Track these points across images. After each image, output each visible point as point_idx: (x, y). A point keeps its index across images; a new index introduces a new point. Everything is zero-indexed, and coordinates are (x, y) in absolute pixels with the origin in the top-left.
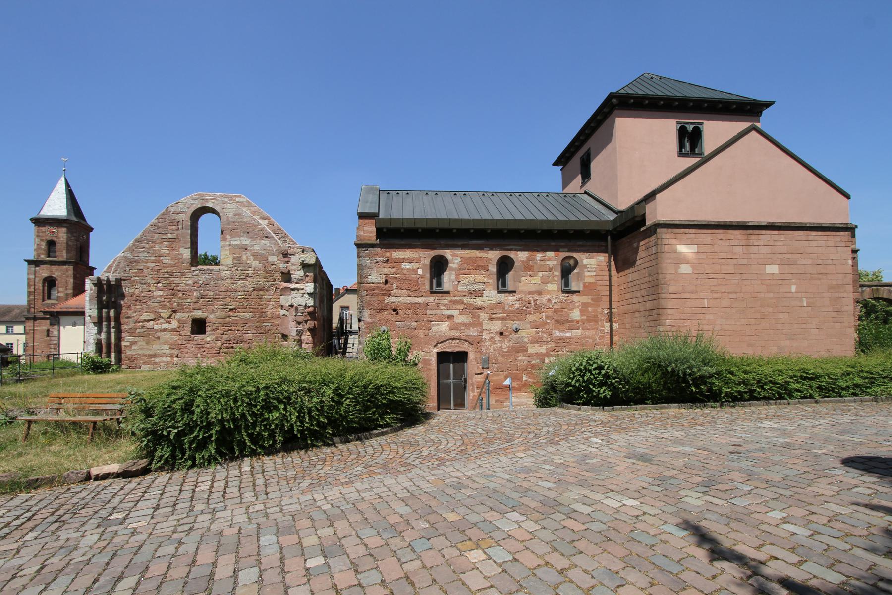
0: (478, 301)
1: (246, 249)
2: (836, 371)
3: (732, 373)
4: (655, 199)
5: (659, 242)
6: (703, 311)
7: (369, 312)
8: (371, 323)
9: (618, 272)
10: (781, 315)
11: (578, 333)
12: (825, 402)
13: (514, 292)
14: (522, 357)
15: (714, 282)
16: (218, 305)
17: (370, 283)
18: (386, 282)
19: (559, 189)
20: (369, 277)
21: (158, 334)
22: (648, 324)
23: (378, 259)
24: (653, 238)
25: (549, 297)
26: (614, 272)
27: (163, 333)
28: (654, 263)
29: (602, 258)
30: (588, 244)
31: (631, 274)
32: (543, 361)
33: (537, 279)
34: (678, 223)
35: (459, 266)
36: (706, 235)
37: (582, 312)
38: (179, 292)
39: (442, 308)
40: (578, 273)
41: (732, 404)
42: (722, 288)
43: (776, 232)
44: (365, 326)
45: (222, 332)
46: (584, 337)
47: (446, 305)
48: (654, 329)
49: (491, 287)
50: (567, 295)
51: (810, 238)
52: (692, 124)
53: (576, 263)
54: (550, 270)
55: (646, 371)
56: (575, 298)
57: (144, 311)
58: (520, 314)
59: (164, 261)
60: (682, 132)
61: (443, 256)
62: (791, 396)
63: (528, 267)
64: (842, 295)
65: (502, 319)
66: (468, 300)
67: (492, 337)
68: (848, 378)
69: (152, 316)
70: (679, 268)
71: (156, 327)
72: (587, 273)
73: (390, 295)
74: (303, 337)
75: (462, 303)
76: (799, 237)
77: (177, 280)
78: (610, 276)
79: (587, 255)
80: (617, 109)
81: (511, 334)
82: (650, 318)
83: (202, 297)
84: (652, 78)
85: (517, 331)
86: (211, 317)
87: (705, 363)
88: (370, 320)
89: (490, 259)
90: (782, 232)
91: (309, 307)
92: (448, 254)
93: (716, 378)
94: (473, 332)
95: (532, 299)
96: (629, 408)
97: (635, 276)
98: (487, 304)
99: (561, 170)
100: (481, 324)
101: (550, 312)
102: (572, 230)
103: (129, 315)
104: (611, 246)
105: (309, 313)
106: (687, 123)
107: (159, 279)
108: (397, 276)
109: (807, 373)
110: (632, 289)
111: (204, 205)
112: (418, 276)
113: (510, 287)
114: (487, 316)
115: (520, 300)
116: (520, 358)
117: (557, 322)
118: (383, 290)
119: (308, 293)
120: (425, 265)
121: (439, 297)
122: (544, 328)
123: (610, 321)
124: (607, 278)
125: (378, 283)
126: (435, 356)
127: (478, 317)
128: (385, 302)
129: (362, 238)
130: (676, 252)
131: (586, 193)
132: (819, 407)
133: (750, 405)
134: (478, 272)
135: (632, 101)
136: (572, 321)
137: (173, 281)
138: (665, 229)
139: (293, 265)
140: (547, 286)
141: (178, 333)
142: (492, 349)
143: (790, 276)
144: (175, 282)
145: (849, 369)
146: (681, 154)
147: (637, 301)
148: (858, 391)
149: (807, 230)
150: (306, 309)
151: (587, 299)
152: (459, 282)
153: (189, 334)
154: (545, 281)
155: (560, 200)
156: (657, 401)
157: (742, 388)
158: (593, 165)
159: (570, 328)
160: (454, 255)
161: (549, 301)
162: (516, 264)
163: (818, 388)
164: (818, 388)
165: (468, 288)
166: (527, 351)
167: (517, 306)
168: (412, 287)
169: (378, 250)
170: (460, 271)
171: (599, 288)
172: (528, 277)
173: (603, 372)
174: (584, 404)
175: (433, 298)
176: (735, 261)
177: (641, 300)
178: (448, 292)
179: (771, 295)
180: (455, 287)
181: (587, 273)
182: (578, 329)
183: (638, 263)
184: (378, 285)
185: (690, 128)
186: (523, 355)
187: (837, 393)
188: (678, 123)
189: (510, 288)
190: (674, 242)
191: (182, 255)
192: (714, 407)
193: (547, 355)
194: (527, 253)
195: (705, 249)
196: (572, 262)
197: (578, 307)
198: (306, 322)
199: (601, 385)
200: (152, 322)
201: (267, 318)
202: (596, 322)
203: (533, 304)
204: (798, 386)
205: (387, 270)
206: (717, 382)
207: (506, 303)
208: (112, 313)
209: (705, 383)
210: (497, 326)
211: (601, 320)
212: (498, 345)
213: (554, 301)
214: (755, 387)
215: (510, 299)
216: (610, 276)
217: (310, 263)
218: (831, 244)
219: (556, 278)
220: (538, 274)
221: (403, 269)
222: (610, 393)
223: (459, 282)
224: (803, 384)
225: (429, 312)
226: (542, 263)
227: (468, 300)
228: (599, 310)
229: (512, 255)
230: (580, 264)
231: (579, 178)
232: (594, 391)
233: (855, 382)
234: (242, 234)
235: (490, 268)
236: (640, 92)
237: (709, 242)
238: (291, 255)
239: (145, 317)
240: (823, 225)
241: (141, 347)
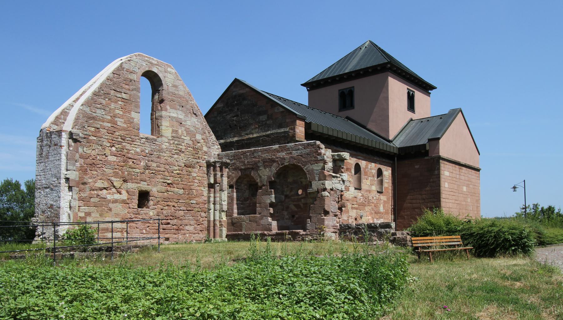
16: (159, 179)
21: (111, 205)
27: (115, 205)
30: (384, 160)
38: (130, 160)
45: (162, 207)
57: (99, 178)
59: (119, 123)
69: (106, 185)
71: (109, 197)
77: (128, 146)
83: (147, 167)
86: (154, 190)
90: (468, 169)
103: (85, 181)
107: (114, 142)
111: (151, 69)
137: (125, 146)
141: (128, 205)
144: (127, 148)
153: (136, 207)
191: (133, 118)
200: (105, 191)
201: (193, 196)
234: (178, 107)
239: (99, 184)
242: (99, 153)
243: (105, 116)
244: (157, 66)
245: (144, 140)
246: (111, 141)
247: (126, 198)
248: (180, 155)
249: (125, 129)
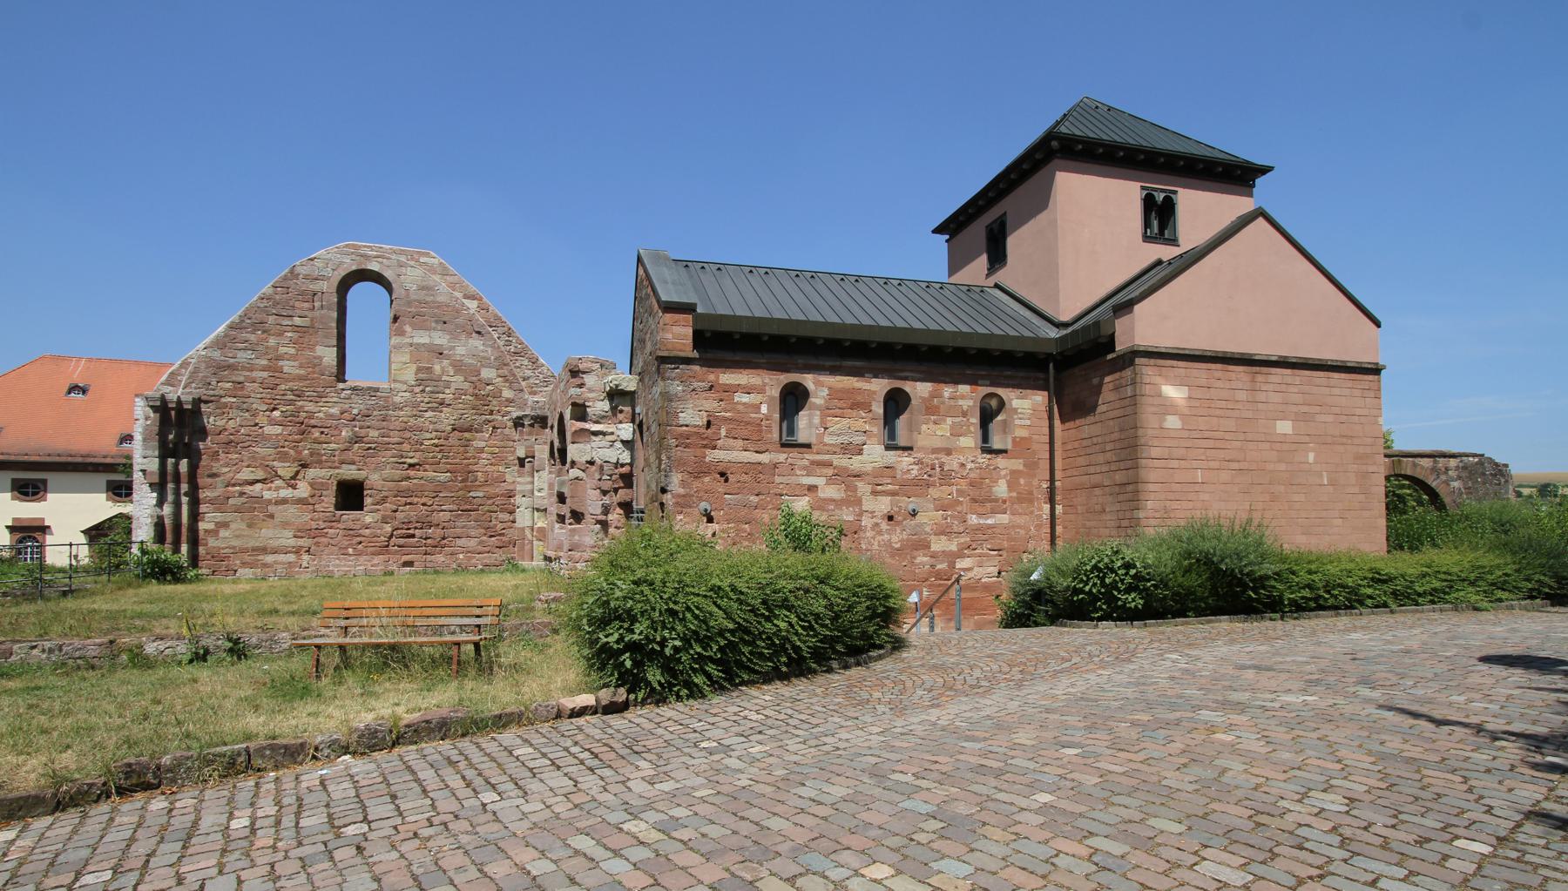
0: (855, 463)
1: (441, 354)
2: (1411, 571)
3: (1293, 573)
4: (1131, 312)
5: (1138, 380)
6: (1197, 487)
7: (680, 476)
8: (684, 496)
9: (1063, 421)
10: (1296, 498)
12: (1401, 611)
13: (911, 449)
14: (922, 558)
15: (1211, 443)
16: (387, 457)
17: (681, 426)
18: (709, 424)
19: (942, 275)
20: (680, 415)
21: (272, 509)
22: (1118, 507)
23: (696, 384)
24: (1128, 373)
25: (962, 460)
26: (1057, 422)
27: (280, 507)
28: (1129, 410)
29: (1039, 398)
30: (1021, 374)
31: (1086, 427)
32: (952, 565)
33: (944, 429)
34: (1163, 350)
35: (826, 402)
36: (1199, 371)
37: (1010, 486)
38: (313, 430)
39: (798, 472)
40: (1004, 421)
41: (1295, 615)
42: (1221, 454)
43: (1289, 371)
44: (674, 500)
45: (394, 507)
46: (1013, 526)
47: (805, 468)
48: (1128, 515)
49: (875, 440)
50: (989, 456)
51: (1333, 382)
52: (1163, 191)
53: (1002, 404)
54: (964, 414)
55: (1188, 570)
56: (1000, 461)
57: (245, 464)
58: (918, 486)
59: (286, 369)
60: (1149, 202)
61: (800, 384)
62: (1362, 603)
63: (931, 409)
64: (1371, 469)
65: (893, 494)
66: (840, 461)
67: (877, 525)
68: (1424, 581)
69: (260, 474)
70: (1165, 420)
71: (267, 495)
72: (1017, 422)
73: (714, 448)
74: (610, 517)
75: (829, 464)
76: (1318, 381)
77: (310, 407)
78: (1051, 427)
79: (1018, 392)
80: (1058, 158)
81: (905, 519)
82: (1121, 498)
83: (357, 439)
84: (1097, 107)
85: (914, 514)
86: (374, 480)
87: (1263, 556)
88: (682, 491)
89: (874, 393)
91: (623, 465)
92: (808, 380)
93: (1275, 579)
94: (847, 515)
95: (936, 461)
96: (1167, 623)
97: (1096, 430)
98: (869, 468)
99: (947, 241)
100: (859, 502)
101: (963, 485)
102: (998, 350)
103: (214, 470)
104: (1055, 379)
105: (622, 476)
106: (1156, 190)
107: (275, 402)
108: (728, 414)
109: (1379, 574)
110: (1089, 451)
111: (363, 267)
112: (761, 416)
113: (902, 441)
114: (869, 488)
115: (919, 462)
116: (919, 560)
117: (974, 500)
118: (704, 439)
119: (622, 441)
120: (772, 398)
121: (794, 453)
122: (955, 510)
123: (1052, 501)
124: (1046, 430)
125: (696, 426)
127: (855, 489)
128: (707, 459)
129: (670, 347)
130: (1160, 395)
131: (997, 286)
132: (1399, 618)
133: (1317, 617)
134: (854, 413)
135: (1080, 147)
136: (996, 500)
137: (302, 407)
138: (1147, 360)
139: (591, 390)
141: (311, 507)
142: (876, 543)
143: (1307, 439)
144: (306, 409)
145: (1424, 569)
146: (1147, 238)
147: (1098, 469)
148: (1436, 597)
149: (1327, 370)
150: (616, 468)
151: (1017, 464)
152: (826, 428)
153: (332, 509)
154: (956, 434)
155: (963, 296)
156: (1200, 613)
157: (1306, 593)
158: (1011, 242)
159: (994, 512)
160: (818, 384)
162: (913, 402)
163: (1392, 593)
164: (1392, 593)
165: (840, 440)
166: (930, 548)
167: (915, 472)
168: (751, 435)
169: (697, 368)
170: (827, 411)
171: (1035, 447)
172: (931, 426)
173: (1133, 572)
174: (1100, 619)
175: (785, 456)
176: (1236, 414)
177: (1105, 468)
178: (808, 446)
179: (1282, 467)
180: (821, 436)
181: (1017, 422)
182: (1005, 513)
183: (1101, 408)
184: (695, 430)
185: (1160, 197)
186: (924, 555)
187: (1413, 600)
188: (1143, 188)
189: (902, 442)
190: (1158, 380)
191: (320, 358)
192: (1274, 620)
193: (960, 555)
194: (929, 384)
195: (1198, 393)
196: (994, 403)
197: (1005, 476)
198: (616, 490)
199: (1128, 590)
200: (258, 486)
201: (477, 483)
202: (1031, 501)
203: (938, 469)
204: (1369, 591)
205: (711, 404)
206: (1278, 585)
207: (899, 467)
208: (184, 465)
209: (1264, 587)
210: (883, 505)
211: (1038, 498)
212: (886, 537)
213: (969, 466)
214: (1321, 593)
215: (904, 461)
216: (1051, 427)
217: (628, 389)
218: (1357, 393)
219: (972, 429)
220: (945, 421)
221: (737, 403)
222: (1141, 602)
223: (826, 428)
224: (1375, 589)
225: (778, 479)
226: (952, 402)
227: (840, 461)
228: (1035, 482)
229: (908, 387)
230: (1007, 406)
231: (983, 259)
232: (1120, 599)
233: (1433, 586)
234: (433, 325)
235: (873, 408)
236: (1092, 135)
237: (1203, 382)
238: (584, 373)
239: (246, 474)
240: (1349, 364)
242: (243, 424)
243: (257, 361)
244: (380, 260)
245: (349, 392)
246: (271, 401)
247: (305, 495)
248: (441, 412)
249: (300, 378)
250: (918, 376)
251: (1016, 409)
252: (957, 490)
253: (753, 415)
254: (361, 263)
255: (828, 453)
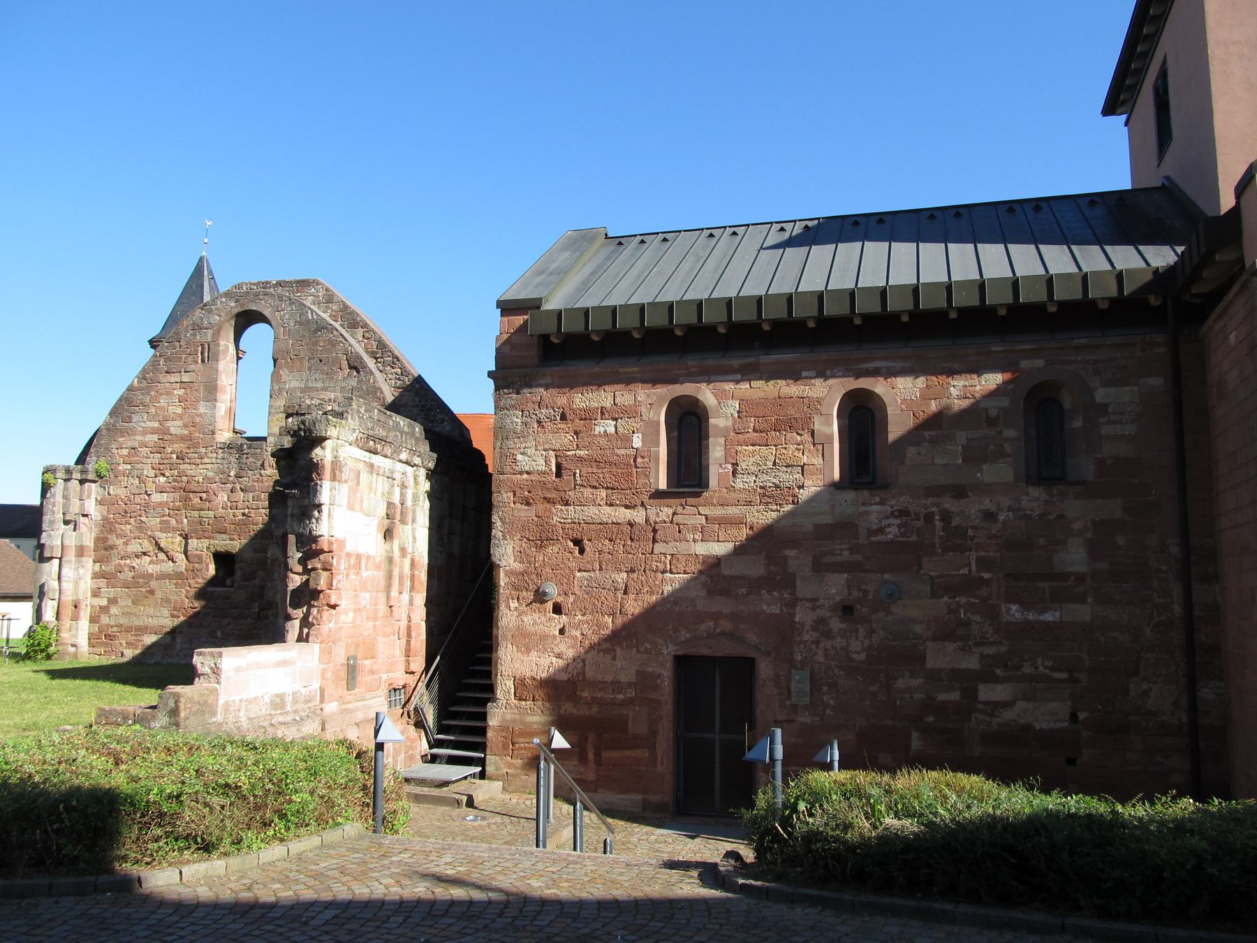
11: (1082, 612)
17: (521, 473)
21: (154, 584)
25: (987, 504)
32: (970, 694)
67: (822, 621)
71: (152, 569)
88: (518, 566)
92: (706, 394)
100: (788, 582)
116: (900, 683)
126: (669, 665)
136: (1065, 576)
140: (981, 471)
142: (820, 653)
161: (989, 516)
166: (922, 659)
193: (985, 675)
205: (564, 439)
210: (835, 587)
212: (839, 642)
219: (1008, 448)
229: (879, 387)
239: (134, 547)
241: (126, 610)
246: (158, 466)
250: (898, 365)
251: (1103, 409)
252: (979, 560)
253: (623, 452)
254: (242, 305)
255: (737, 503)
